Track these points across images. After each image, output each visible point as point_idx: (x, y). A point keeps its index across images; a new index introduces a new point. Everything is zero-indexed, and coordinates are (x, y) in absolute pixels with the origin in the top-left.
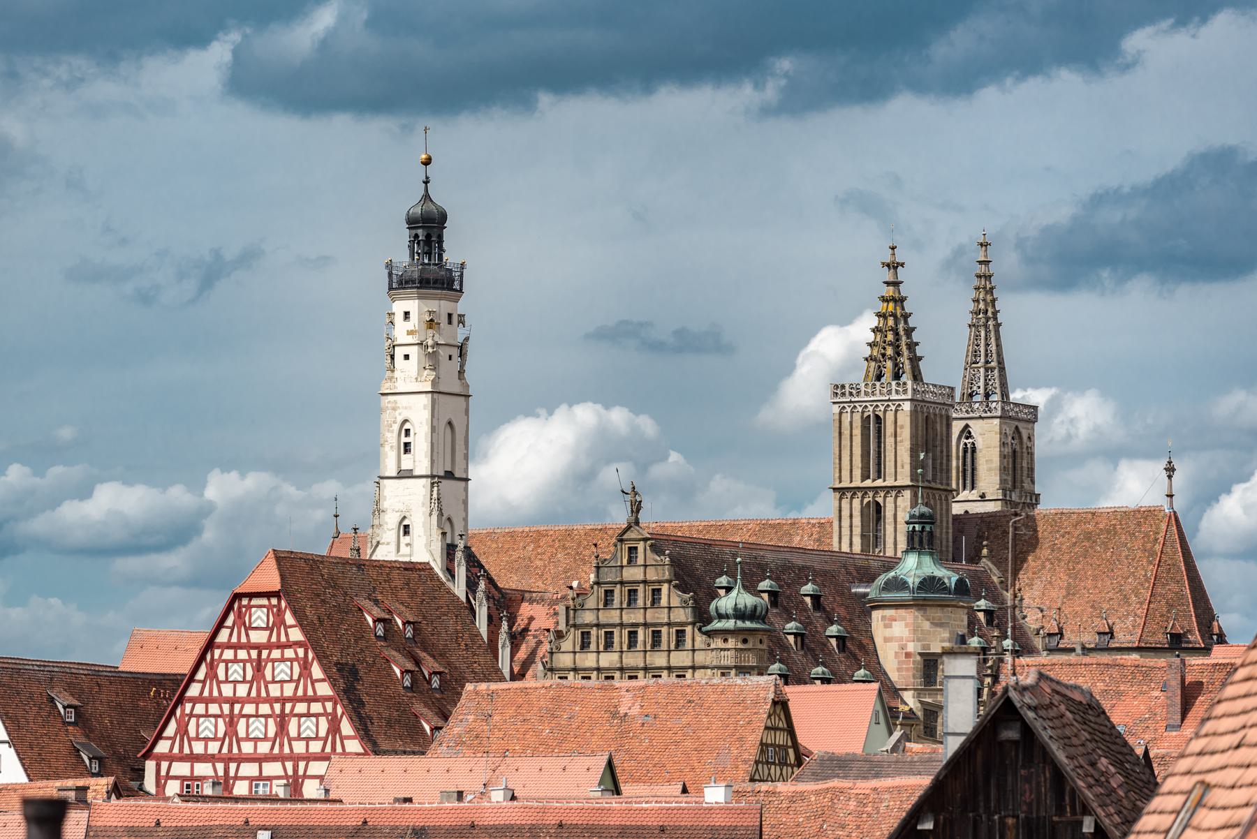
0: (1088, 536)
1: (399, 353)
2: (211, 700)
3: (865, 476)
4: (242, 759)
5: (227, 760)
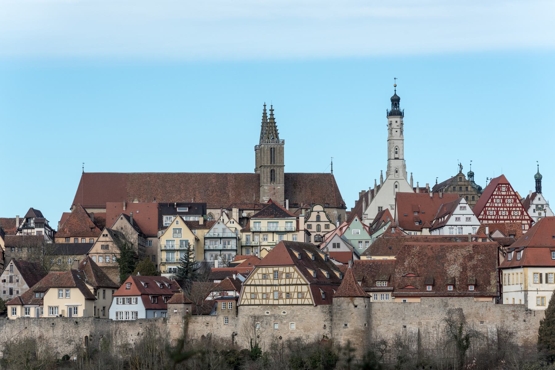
0: (312, 180)
1: (394, 131)
2: (492, 207)
3: (271, 163)
4: (500, 220)
5: (496, 220)
